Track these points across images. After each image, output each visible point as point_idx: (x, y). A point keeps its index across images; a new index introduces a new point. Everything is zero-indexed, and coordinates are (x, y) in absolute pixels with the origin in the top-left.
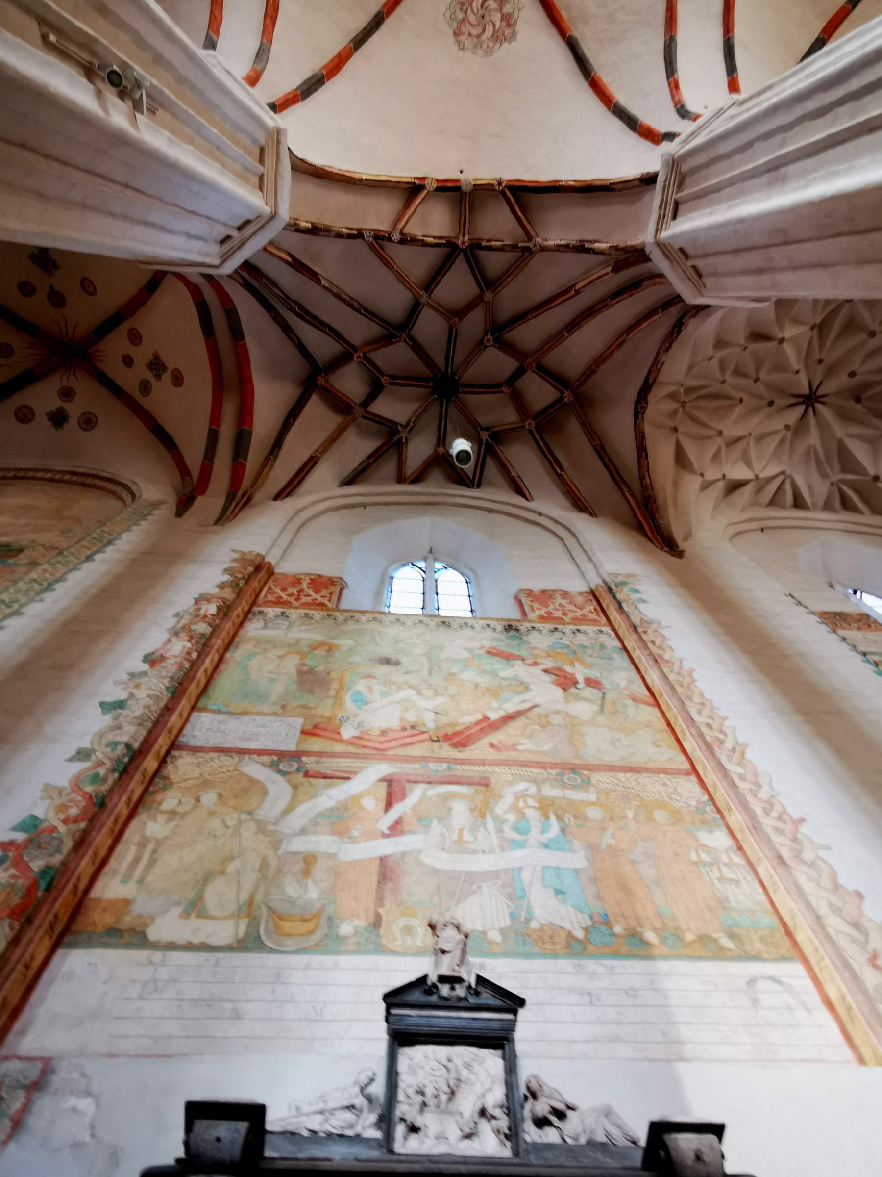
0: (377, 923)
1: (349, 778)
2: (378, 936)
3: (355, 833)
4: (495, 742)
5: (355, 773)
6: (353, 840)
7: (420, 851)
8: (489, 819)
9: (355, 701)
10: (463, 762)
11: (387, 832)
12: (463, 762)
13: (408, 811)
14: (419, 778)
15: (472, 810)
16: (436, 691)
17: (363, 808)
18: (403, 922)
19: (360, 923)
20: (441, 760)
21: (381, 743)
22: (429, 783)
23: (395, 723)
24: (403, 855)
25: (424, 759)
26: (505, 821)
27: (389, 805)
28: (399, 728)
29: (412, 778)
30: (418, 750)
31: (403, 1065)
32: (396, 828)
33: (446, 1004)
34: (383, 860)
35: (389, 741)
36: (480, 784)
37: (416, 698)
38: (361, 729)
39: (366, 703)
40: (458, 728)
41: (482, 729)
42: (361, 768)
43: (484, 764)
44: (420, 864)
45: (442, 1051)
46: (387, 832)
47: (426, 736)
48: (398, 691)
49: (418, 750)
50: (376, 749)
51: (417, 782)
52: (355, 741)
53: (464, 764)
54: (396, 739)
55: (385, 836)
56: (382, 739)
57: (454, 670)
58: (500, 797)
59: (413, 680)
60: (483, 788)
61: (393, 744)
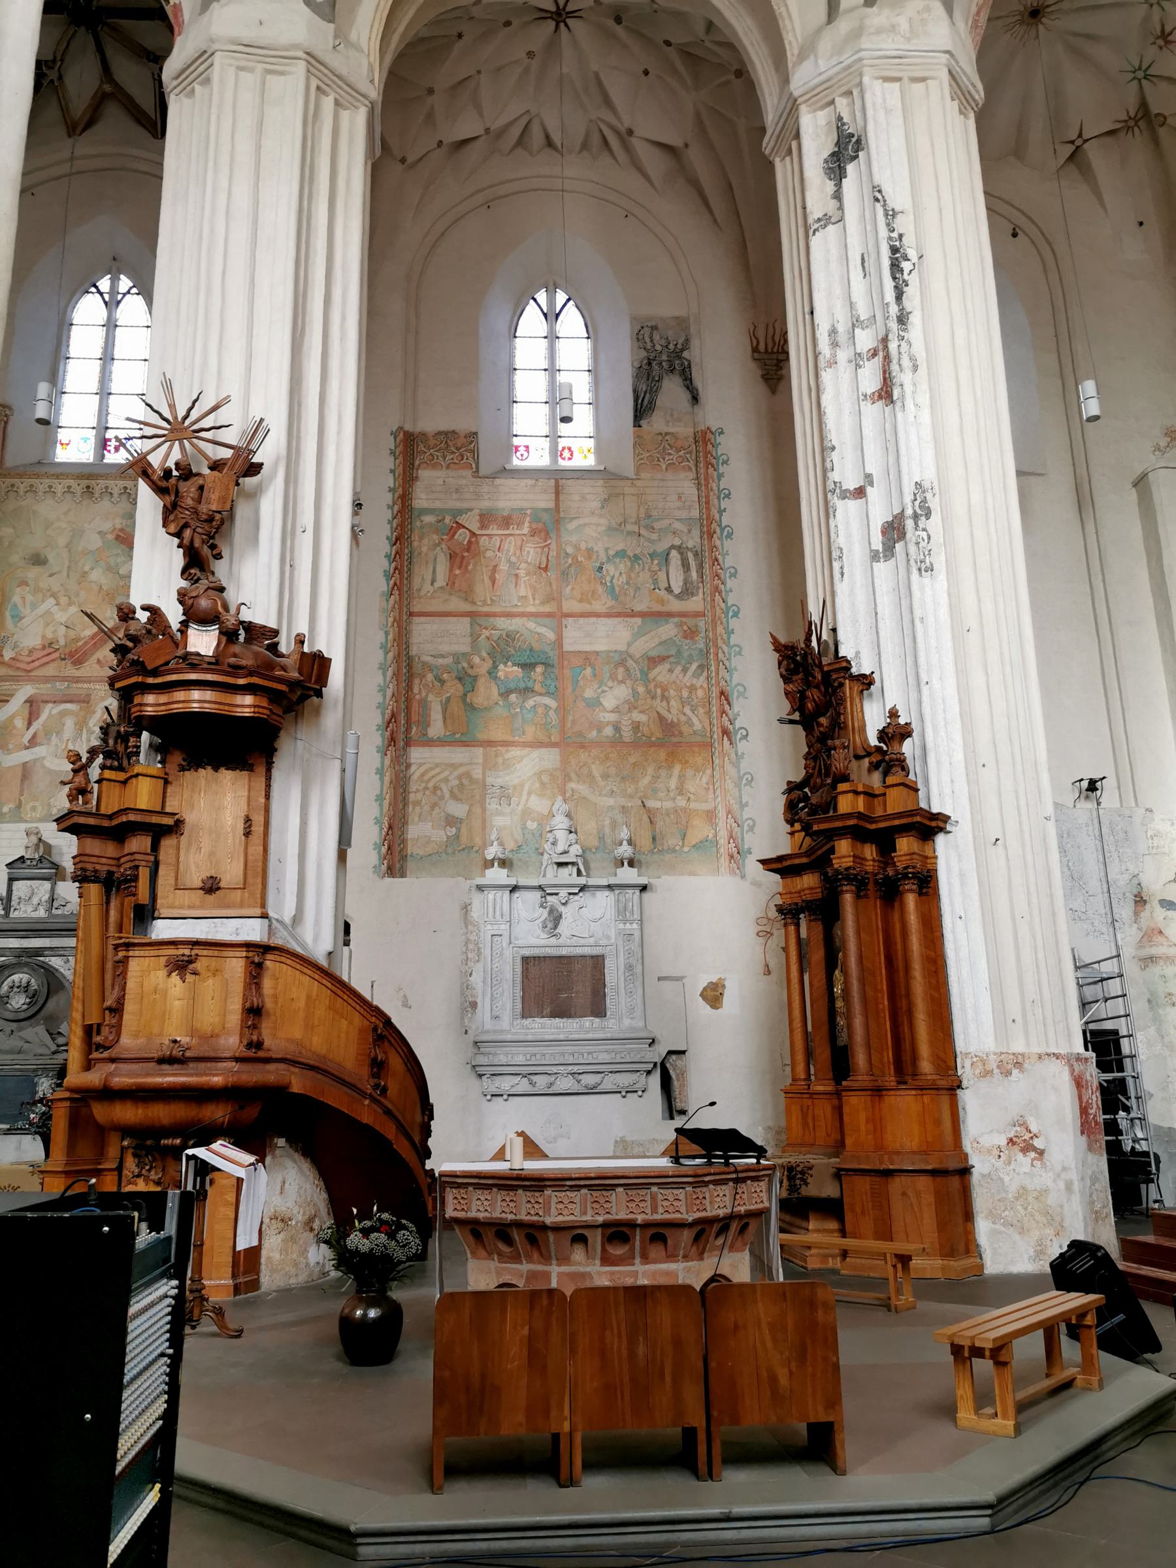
0: (19, 806)
1: (7, 701)
2: (20, 813)
3: (11, 746)
4: (101, 658)
5: (12, 695)
6: (9, 752)
7: (44, 758)
8: (85, 731)
9: (12, 617)
10: (77, 680)
11: (27, 744)
12: (77, 680)
13: (41, 727)
14: (49, 698)
15: (76, 725)
16: (70, 598)
17: (15, 727)
18: (31, 804)
19: (12, 806)
20: (64, 679)
21: (29, 663)
22: (55, 702)
23: (36, 642)
24: (35, 760)
25: (53, 679)
26: (93, 732)
27: (29, 724)
28: (40, 647)
29: (44, 698)
30: (50, 670)
31: (14, 888)
32: (33, 742)
33: (29, 867)
34: (25, 764)
35: (33, 661)
36: (84, 702)
37: (55, 609)
38: (16, 650)
39: (21, 619)
40: (80, 644)
41: (95, 643)
42: (16, 690)
43: (90, 682)
44: (43, 767)
45: (29, 882)
46: (27, 744)
47: (56, 655)
48: (43, 601)
49: (50, 670)
50: (25, 670)
51: (47, 702)
52: (13, 663)
53: (77, 682)
54: (38, 659)
55: (27, 748)
56: (30, 659)
57: (87, 568)
58: (94, 712)
59: (55, 584)
60: (85, 705)
61: (37, 664)
